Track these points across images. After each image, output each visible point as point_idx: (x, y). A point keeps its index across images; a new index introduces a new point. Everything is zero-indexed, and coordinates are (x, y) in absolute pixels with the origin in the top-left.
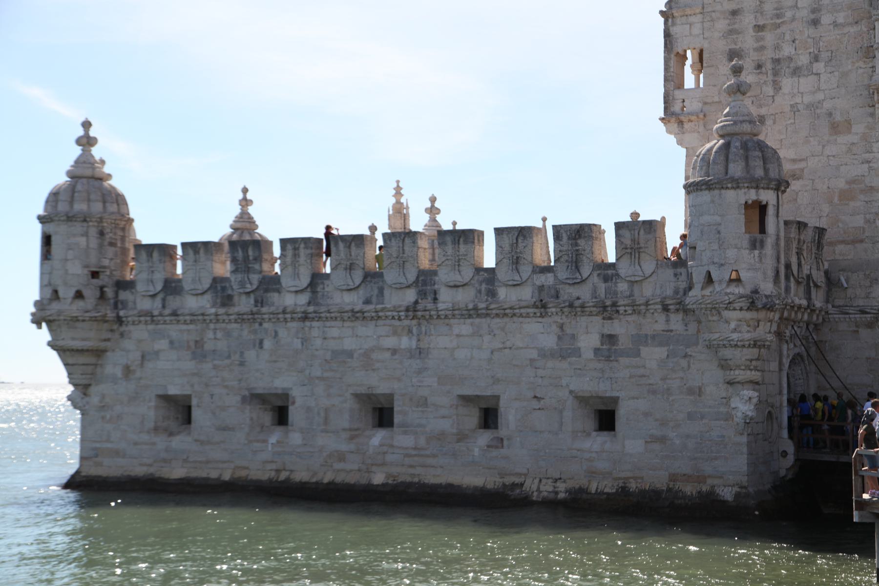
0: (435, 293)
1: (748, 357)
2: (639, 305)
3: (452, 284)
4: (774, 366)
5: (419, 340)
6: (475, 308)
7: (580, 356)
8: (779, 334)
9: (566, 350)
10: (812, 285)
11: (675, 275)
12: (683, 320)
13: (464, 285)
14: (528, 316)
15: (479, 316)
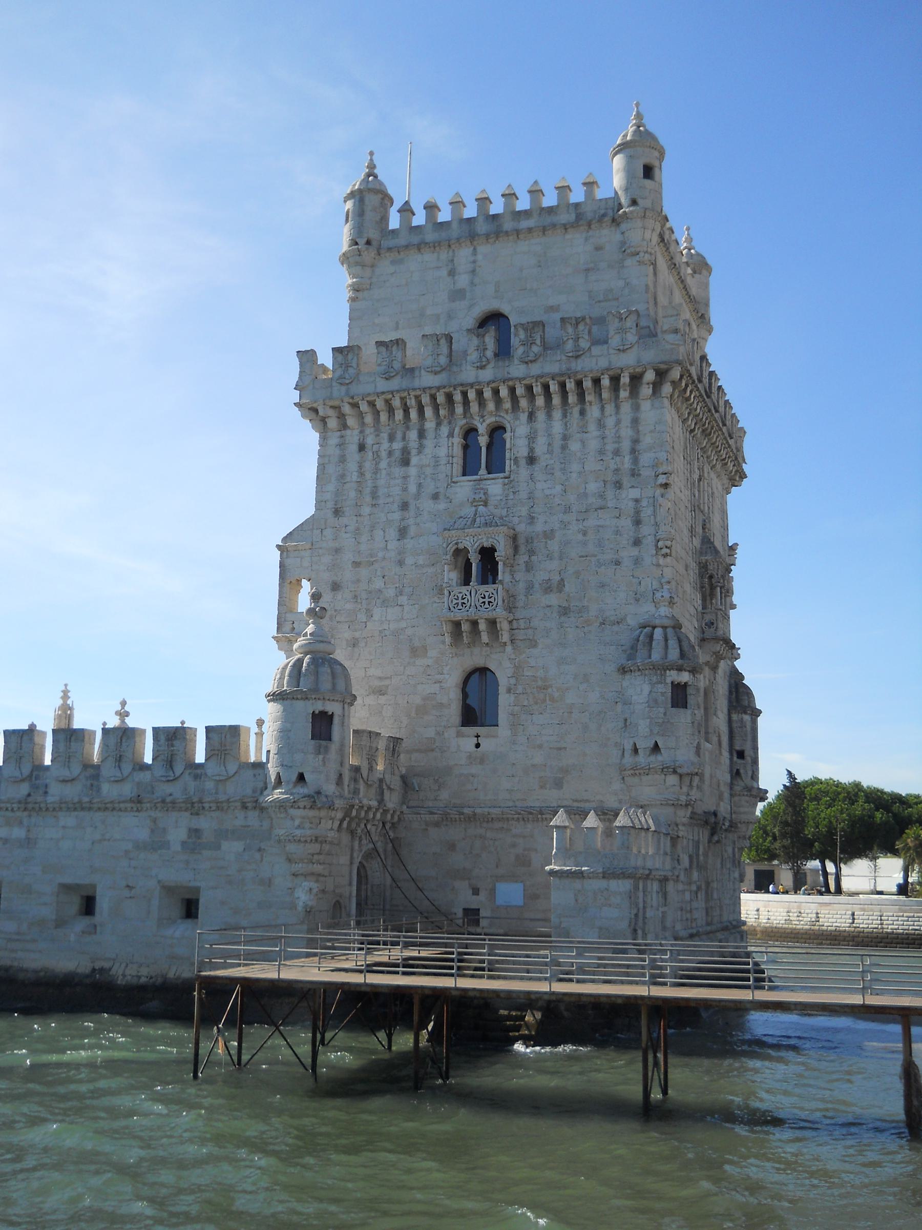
0: (46, 786)
1: (310, 851)
2: (222, 802)
3: (61, 779)
4: (344, 860)
5: (29, 831)
6: (80, 802)
7: (169, 849)
8: (352, 833)
9: (157, 844)
10: (385, 787)
11: (255, 775)
12: (259, 816)
13: (73, 780)
14: (126, 810)
15: (83, 809)
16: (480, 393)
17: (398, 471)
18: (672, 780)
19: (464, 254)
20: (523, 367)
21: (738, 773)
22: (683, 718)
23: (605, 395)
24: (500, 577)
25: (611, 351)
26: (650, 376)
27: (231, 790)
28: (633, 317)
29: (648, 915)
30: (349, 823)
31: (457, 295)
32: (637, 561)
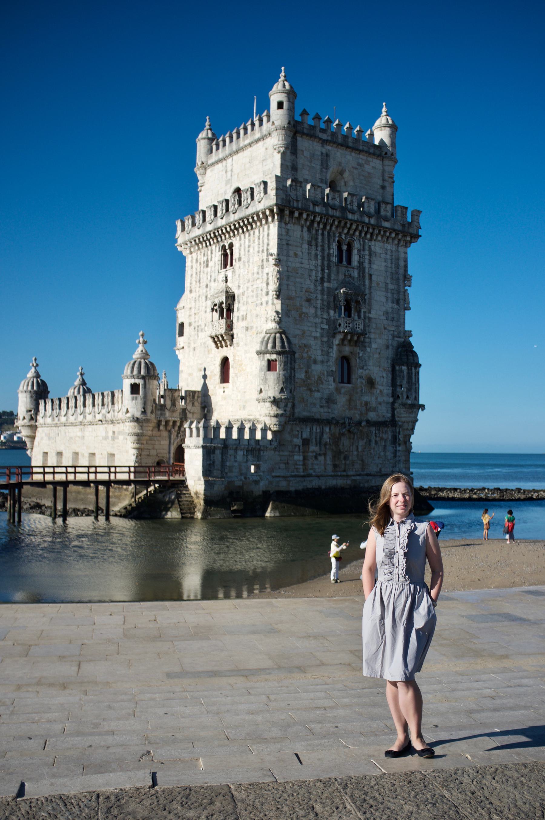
4: (165, 443)
10: (187, 411)
16: (222, 230)
17: (206, 270)
18: (268, 404)
19: (229, 160)
20: (233, 215)
21: (398, 397)
22: (272, 376)
23: (258, 224)
24: (225, 316)
25: (257, 203)
26: (268, 213)
27: (120, 416)
28: (262, 186)
29: (228, 464)
30: (166, 429)
31: (228, 182)
32: (267, 303)
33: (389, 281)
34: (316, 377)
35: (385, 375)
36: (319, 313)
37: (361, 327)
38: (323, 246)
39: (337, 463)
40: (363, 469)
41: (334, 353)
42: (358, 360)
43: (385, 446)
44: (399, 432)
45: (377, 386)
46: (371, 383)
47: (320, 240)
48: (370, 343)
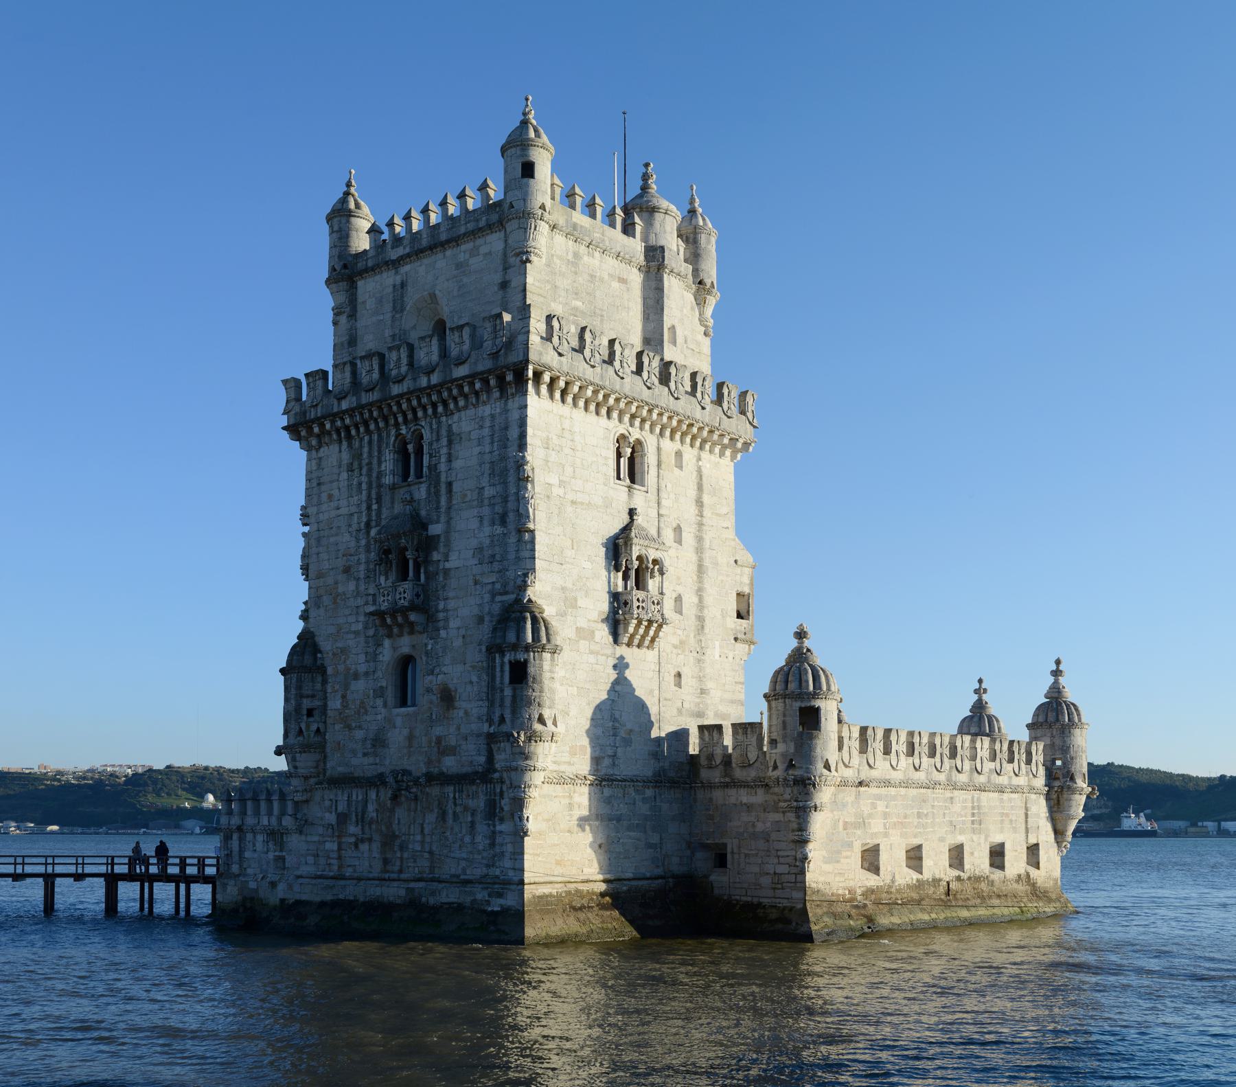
33: (485, 482)
34: (358, 702)
35: (474, 679)
36: (362, 587)
37: (408, 596)
38: (370, 464)
39: (388, 856)
40: (432, 868)
41: (387, 653)
42: (424, 658)
43: (473, 823)
44: (502, 793)
45: (457, 704)
46: (447, 697)
47: (365, 455)
48: (446, 620)
